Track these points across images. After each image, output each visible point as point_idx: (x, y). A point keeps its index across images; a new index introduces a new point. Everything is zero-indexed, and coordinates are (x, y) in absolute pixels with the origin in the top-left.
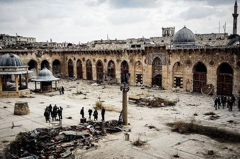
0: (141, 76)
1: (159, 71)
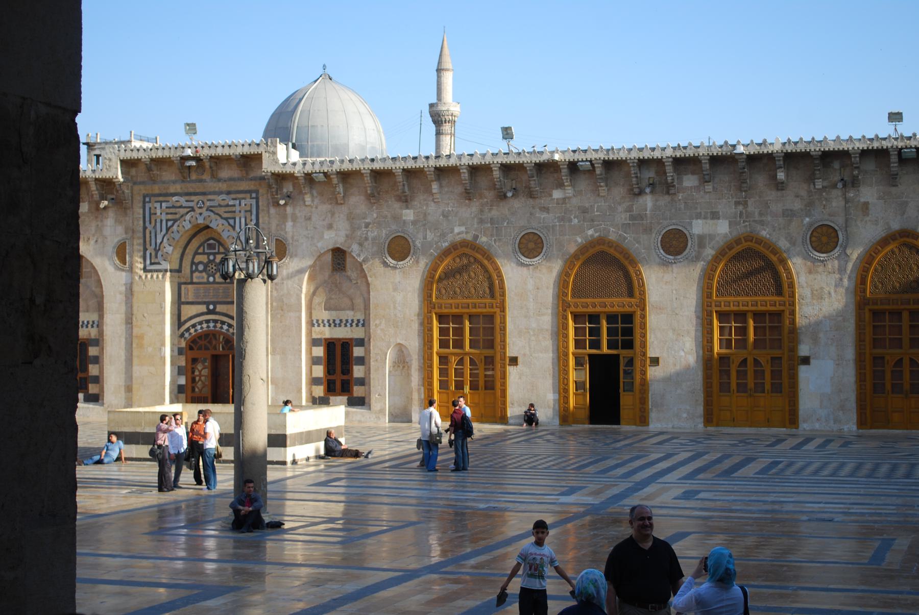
1: (210, 312)
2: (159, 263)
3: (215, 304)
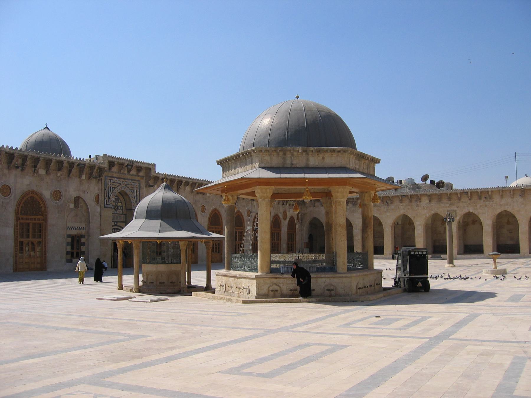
0: (83, 240)
3: (117, 222)
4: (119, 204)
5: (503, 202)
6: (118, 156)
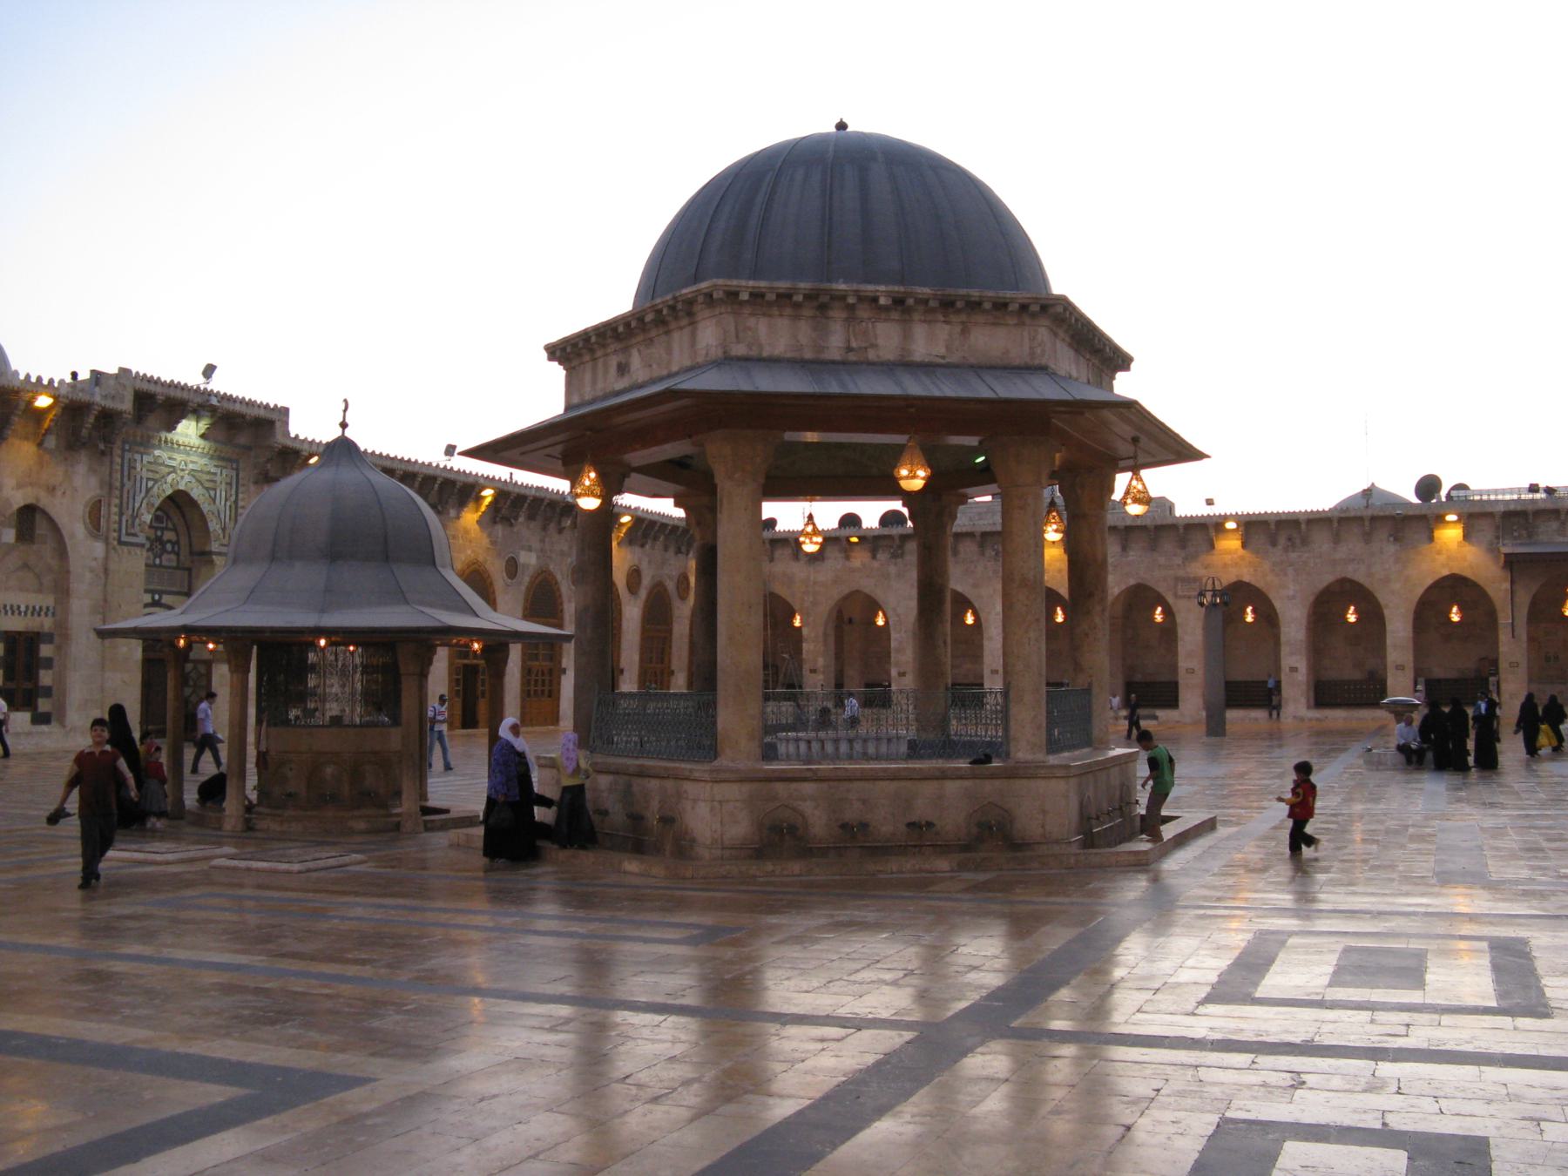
2: (135, 535)
3: (161, 593)
4: (169, 535)
5: (1342, 552)
6: (166, 377)
